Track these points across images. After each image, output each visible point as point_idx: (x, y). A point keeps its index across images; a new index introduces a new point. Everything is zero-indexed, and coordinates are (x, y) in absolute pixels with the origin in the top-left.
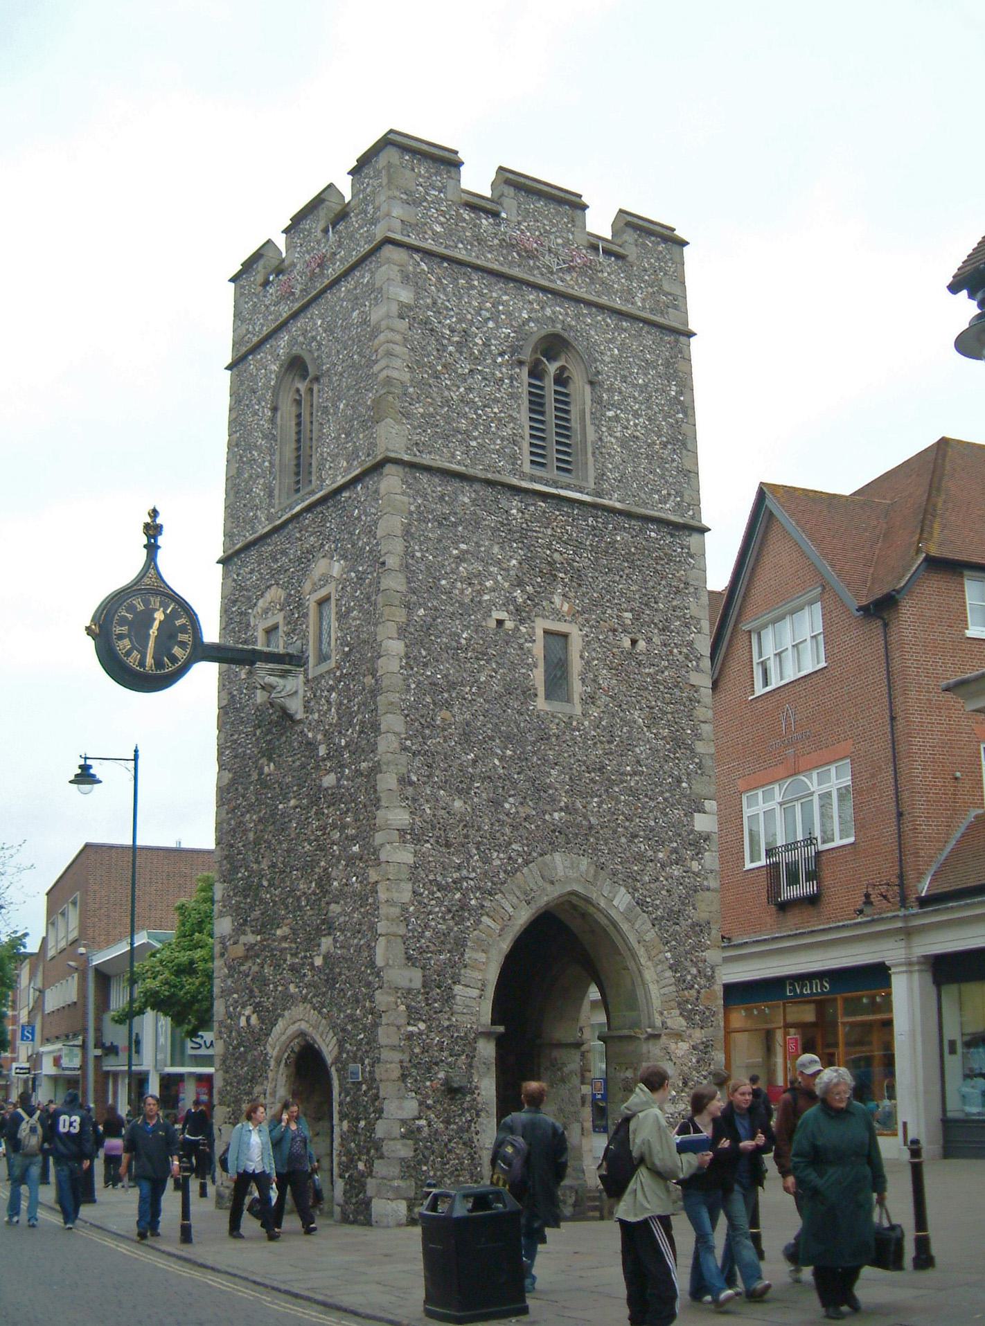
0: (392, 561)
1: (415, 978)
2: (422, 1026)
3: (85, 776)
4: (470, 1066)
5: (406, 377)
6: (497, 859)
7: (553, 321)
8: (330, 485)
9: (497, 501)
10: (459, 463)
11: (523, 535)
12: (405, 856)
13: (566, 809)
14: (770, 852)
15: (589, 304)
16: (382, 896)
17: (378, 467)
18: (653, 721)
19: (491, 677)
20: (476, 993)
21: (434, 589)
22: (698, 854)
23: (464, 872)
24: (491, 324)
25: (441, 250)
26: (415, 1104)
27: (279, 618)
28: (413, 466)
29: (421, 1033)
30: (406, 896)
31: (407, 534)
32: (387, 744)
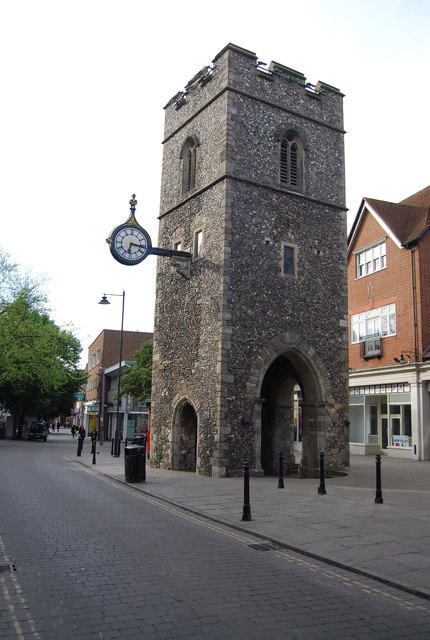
1: (231, 379)
3: (104, 301)
6: (264, 333)
7: (291, 124)
8: (204, 186)
11: (277, 209)
13: (292, 316)
14: (361, 338)
15: (305, 118)
18: (325, 283)
20: (254, 385)
21: (243, 228)
22: (341, 335)
27: (182, 239)
28: (235, 179)
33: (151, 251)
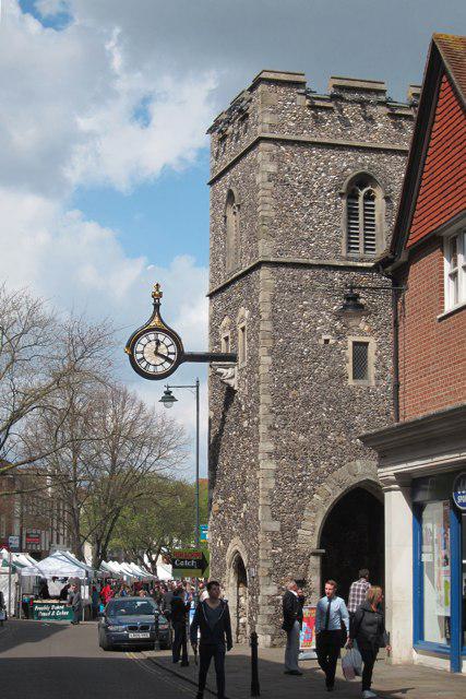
0: (265, 316)
1: (276, 526)
2: (280, 550)
4: (307, 570)
5: (273, 214)
6: (323, 465)
9: (326, 275)
10: (303, 257)
12: (272, 466)
15: (386, 151)
16: (261, 485)
17: (258, 266)
19: (323, 371)
23: (304, 473)
24: (323, 175)
25: (293, 137)
26: (276, 588)
29: (279, 553)
30: (272, 486)
31: (273, 300)
32: (262, 409)
33: (183, 357)
